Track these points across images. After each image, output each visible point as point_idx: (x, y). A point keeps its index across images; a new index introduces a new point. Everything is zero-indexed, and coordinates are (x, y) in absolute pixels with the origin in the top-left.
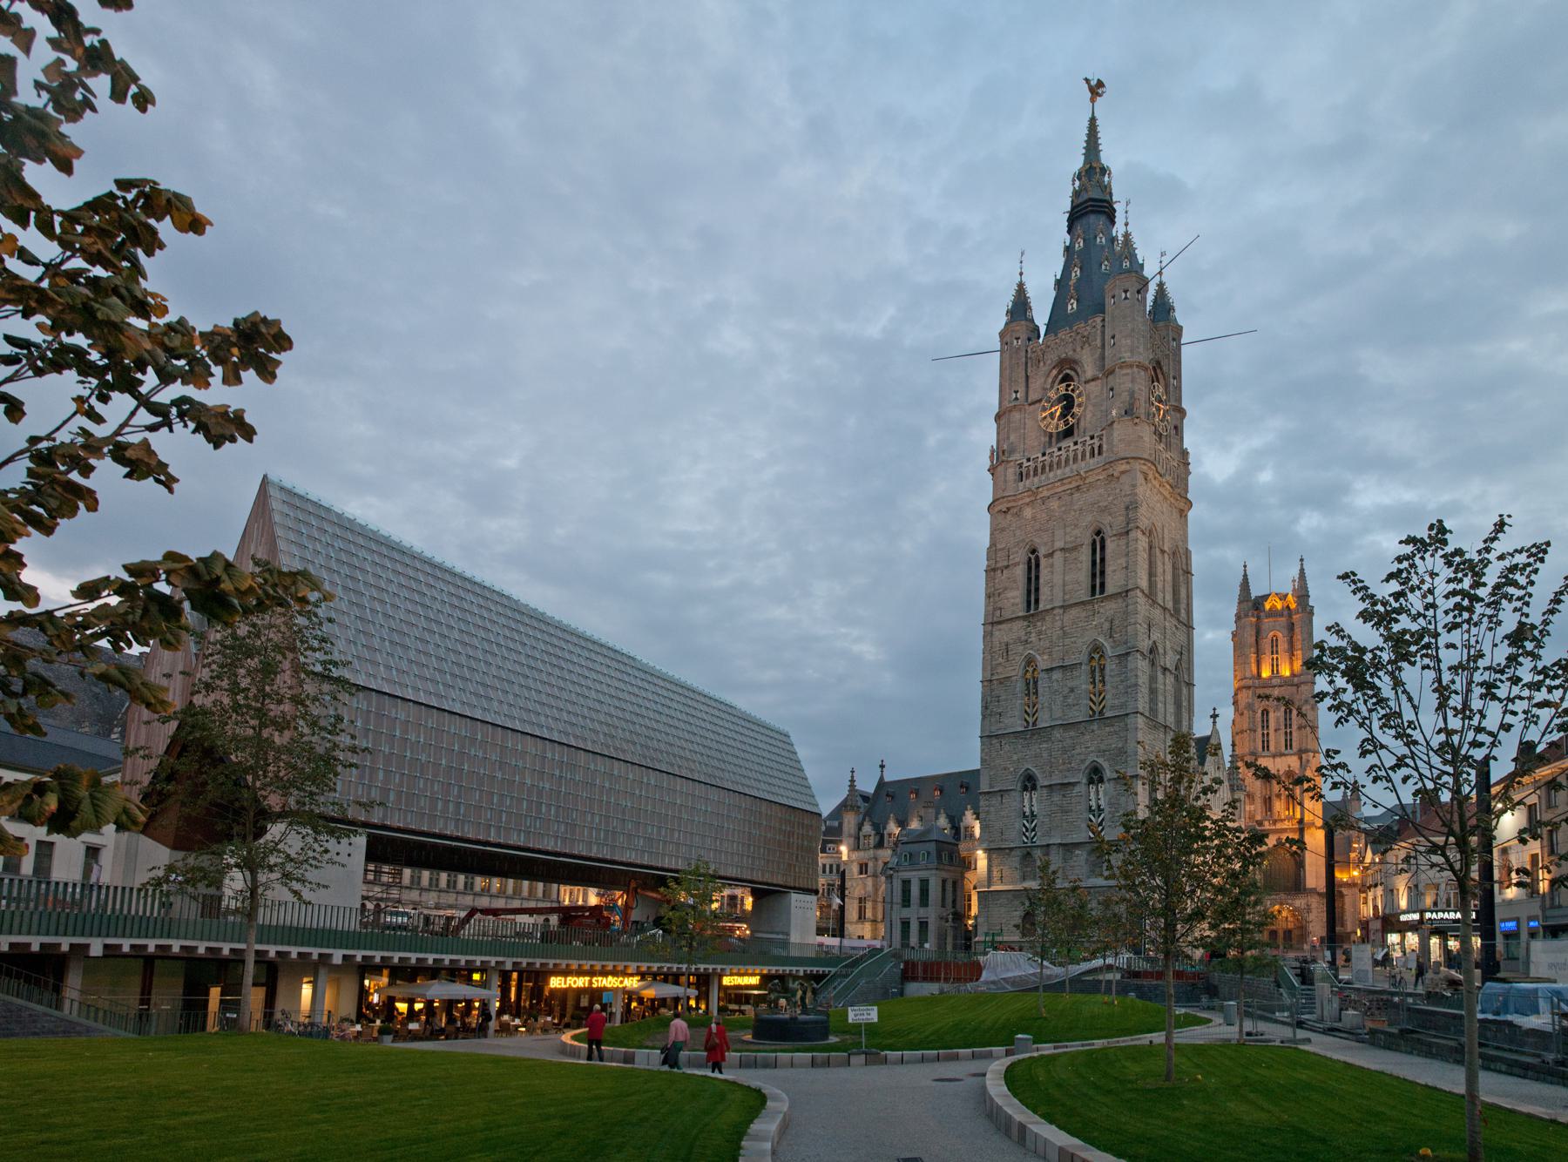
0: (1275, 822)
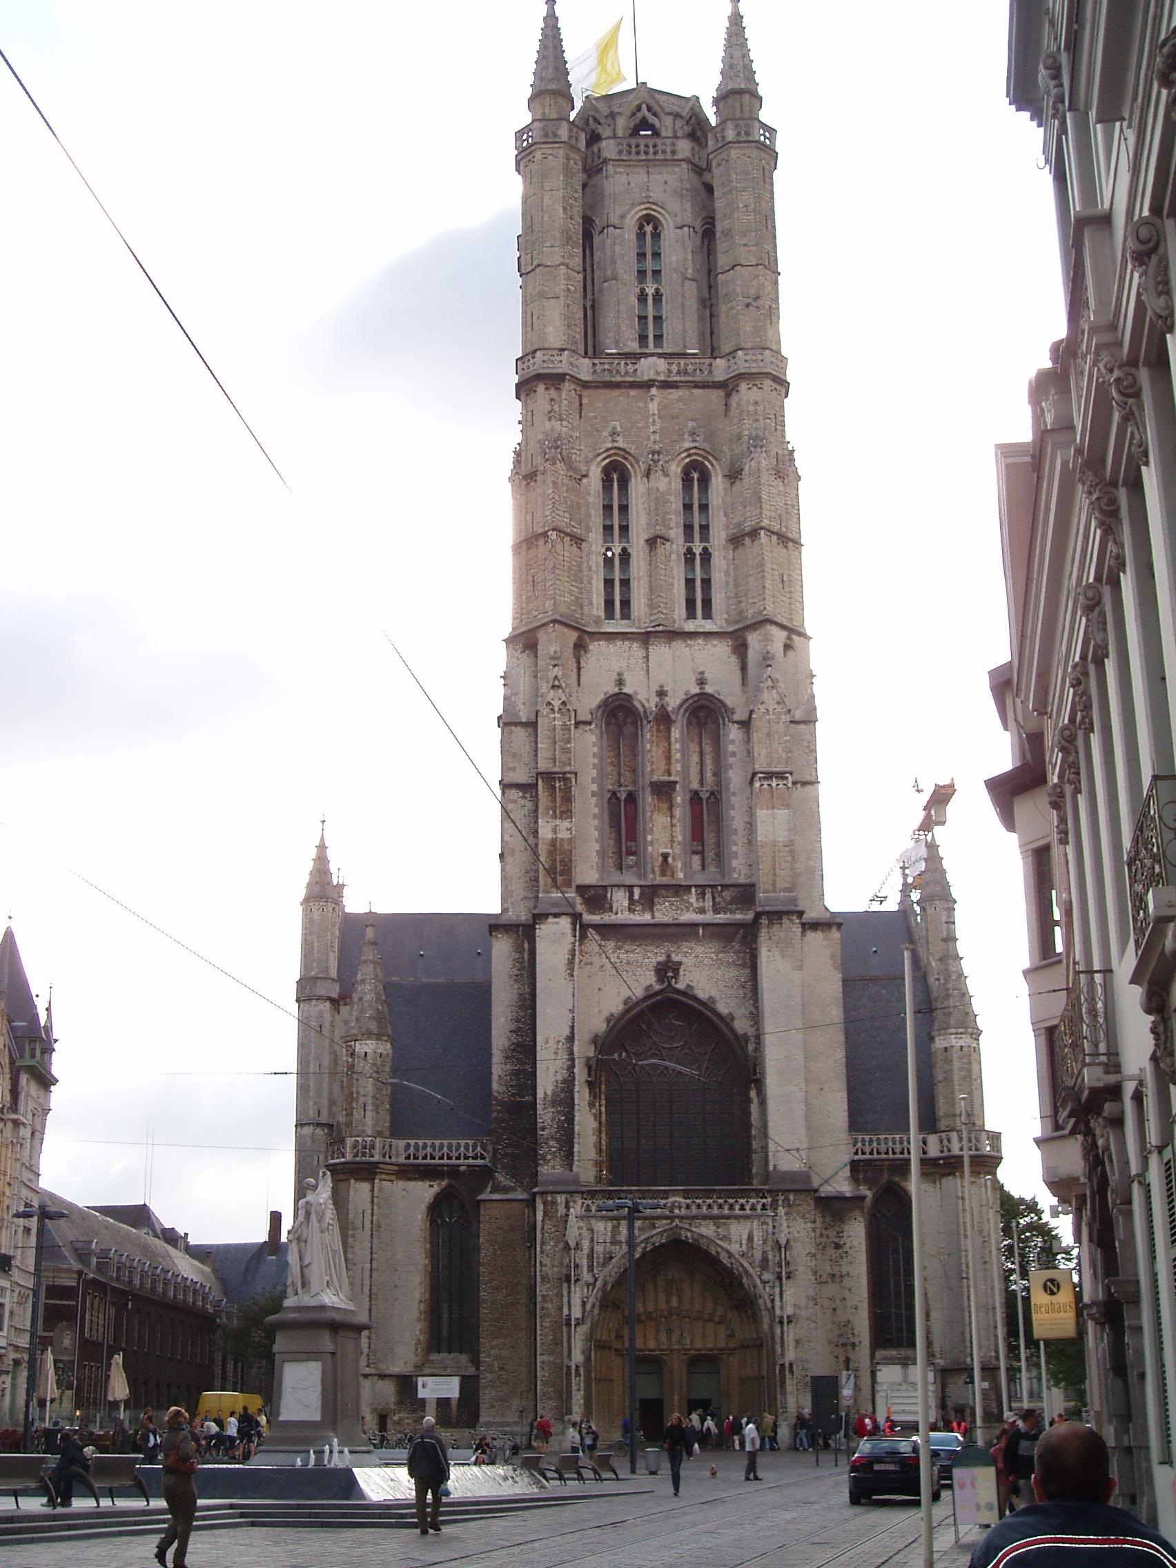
0: (650, 896)
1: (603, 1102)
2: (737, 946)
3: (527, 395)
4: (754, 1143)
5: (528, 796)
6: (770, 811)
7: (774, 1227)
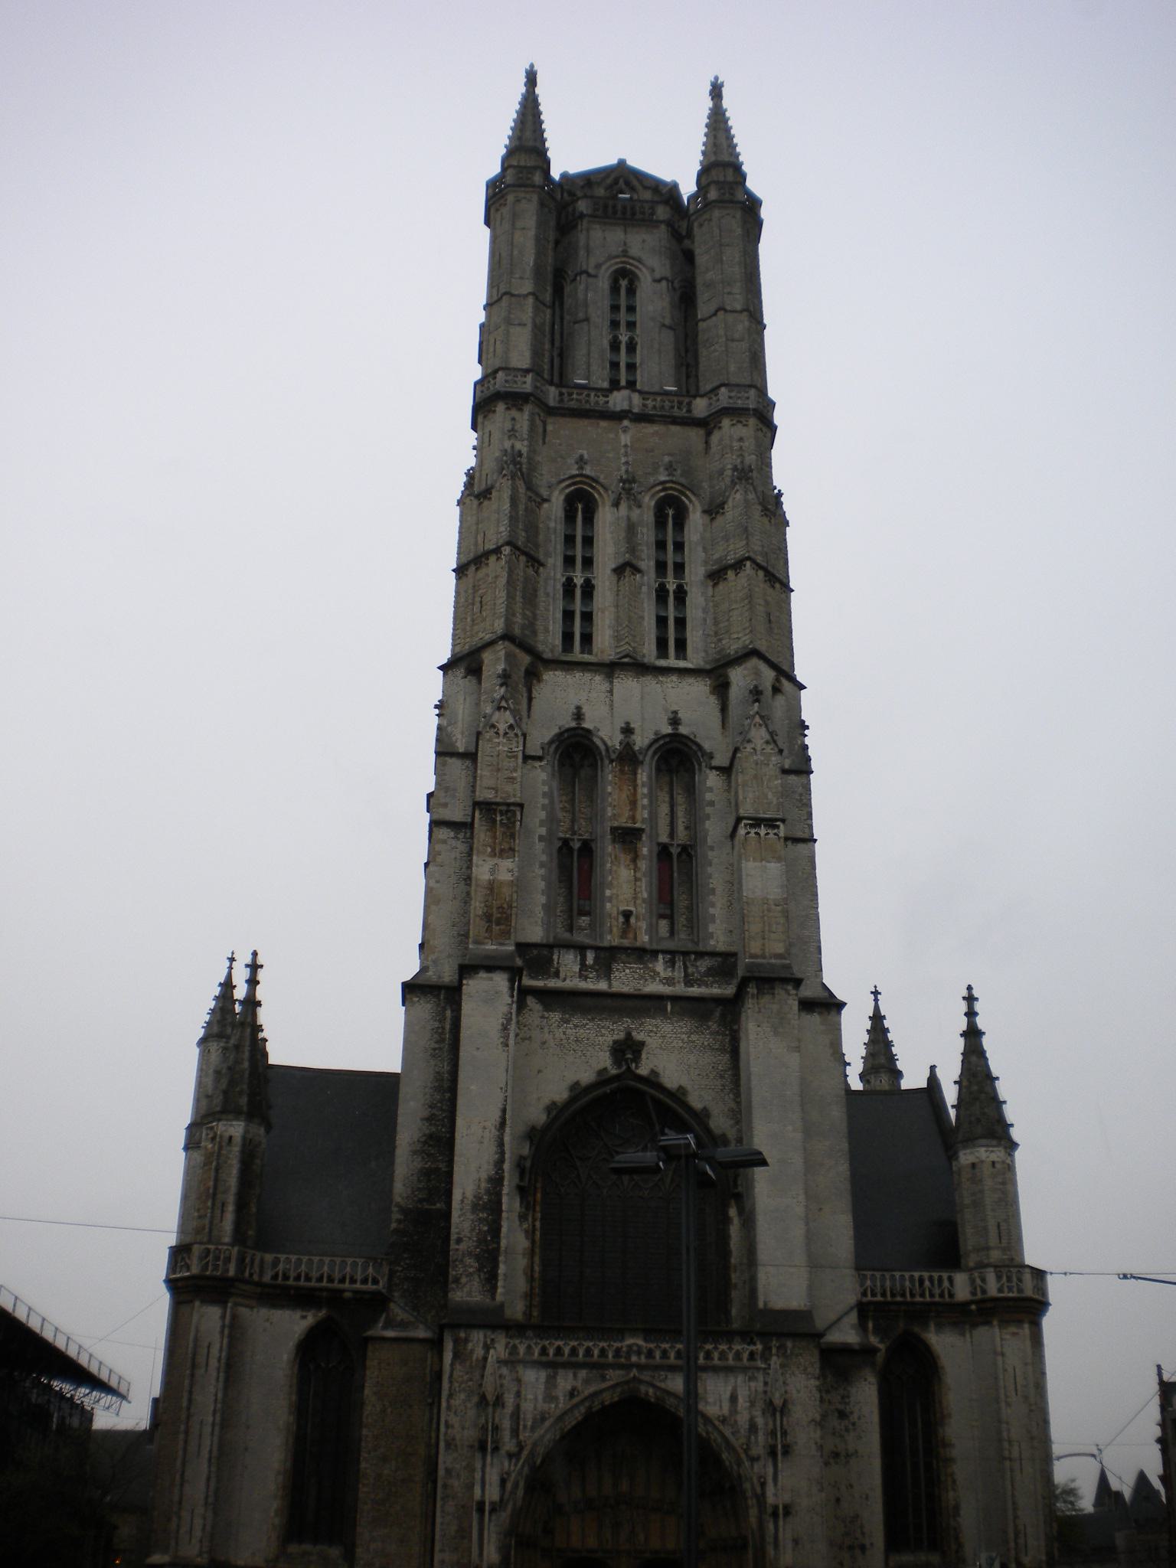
0: (608, 958)
1: (539, 1215)
2: (714, 1027)
3: (485, 417)
4: (733, 1276)
5: (461, 836)
6: (758, 864)
7: (766, 1384)
